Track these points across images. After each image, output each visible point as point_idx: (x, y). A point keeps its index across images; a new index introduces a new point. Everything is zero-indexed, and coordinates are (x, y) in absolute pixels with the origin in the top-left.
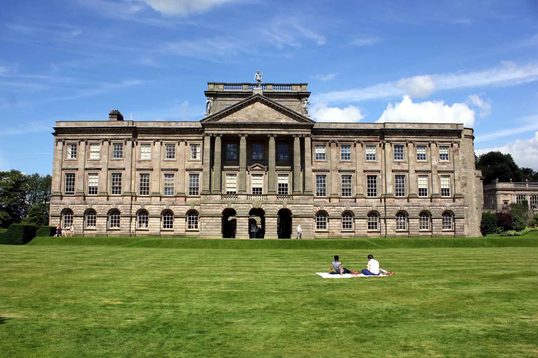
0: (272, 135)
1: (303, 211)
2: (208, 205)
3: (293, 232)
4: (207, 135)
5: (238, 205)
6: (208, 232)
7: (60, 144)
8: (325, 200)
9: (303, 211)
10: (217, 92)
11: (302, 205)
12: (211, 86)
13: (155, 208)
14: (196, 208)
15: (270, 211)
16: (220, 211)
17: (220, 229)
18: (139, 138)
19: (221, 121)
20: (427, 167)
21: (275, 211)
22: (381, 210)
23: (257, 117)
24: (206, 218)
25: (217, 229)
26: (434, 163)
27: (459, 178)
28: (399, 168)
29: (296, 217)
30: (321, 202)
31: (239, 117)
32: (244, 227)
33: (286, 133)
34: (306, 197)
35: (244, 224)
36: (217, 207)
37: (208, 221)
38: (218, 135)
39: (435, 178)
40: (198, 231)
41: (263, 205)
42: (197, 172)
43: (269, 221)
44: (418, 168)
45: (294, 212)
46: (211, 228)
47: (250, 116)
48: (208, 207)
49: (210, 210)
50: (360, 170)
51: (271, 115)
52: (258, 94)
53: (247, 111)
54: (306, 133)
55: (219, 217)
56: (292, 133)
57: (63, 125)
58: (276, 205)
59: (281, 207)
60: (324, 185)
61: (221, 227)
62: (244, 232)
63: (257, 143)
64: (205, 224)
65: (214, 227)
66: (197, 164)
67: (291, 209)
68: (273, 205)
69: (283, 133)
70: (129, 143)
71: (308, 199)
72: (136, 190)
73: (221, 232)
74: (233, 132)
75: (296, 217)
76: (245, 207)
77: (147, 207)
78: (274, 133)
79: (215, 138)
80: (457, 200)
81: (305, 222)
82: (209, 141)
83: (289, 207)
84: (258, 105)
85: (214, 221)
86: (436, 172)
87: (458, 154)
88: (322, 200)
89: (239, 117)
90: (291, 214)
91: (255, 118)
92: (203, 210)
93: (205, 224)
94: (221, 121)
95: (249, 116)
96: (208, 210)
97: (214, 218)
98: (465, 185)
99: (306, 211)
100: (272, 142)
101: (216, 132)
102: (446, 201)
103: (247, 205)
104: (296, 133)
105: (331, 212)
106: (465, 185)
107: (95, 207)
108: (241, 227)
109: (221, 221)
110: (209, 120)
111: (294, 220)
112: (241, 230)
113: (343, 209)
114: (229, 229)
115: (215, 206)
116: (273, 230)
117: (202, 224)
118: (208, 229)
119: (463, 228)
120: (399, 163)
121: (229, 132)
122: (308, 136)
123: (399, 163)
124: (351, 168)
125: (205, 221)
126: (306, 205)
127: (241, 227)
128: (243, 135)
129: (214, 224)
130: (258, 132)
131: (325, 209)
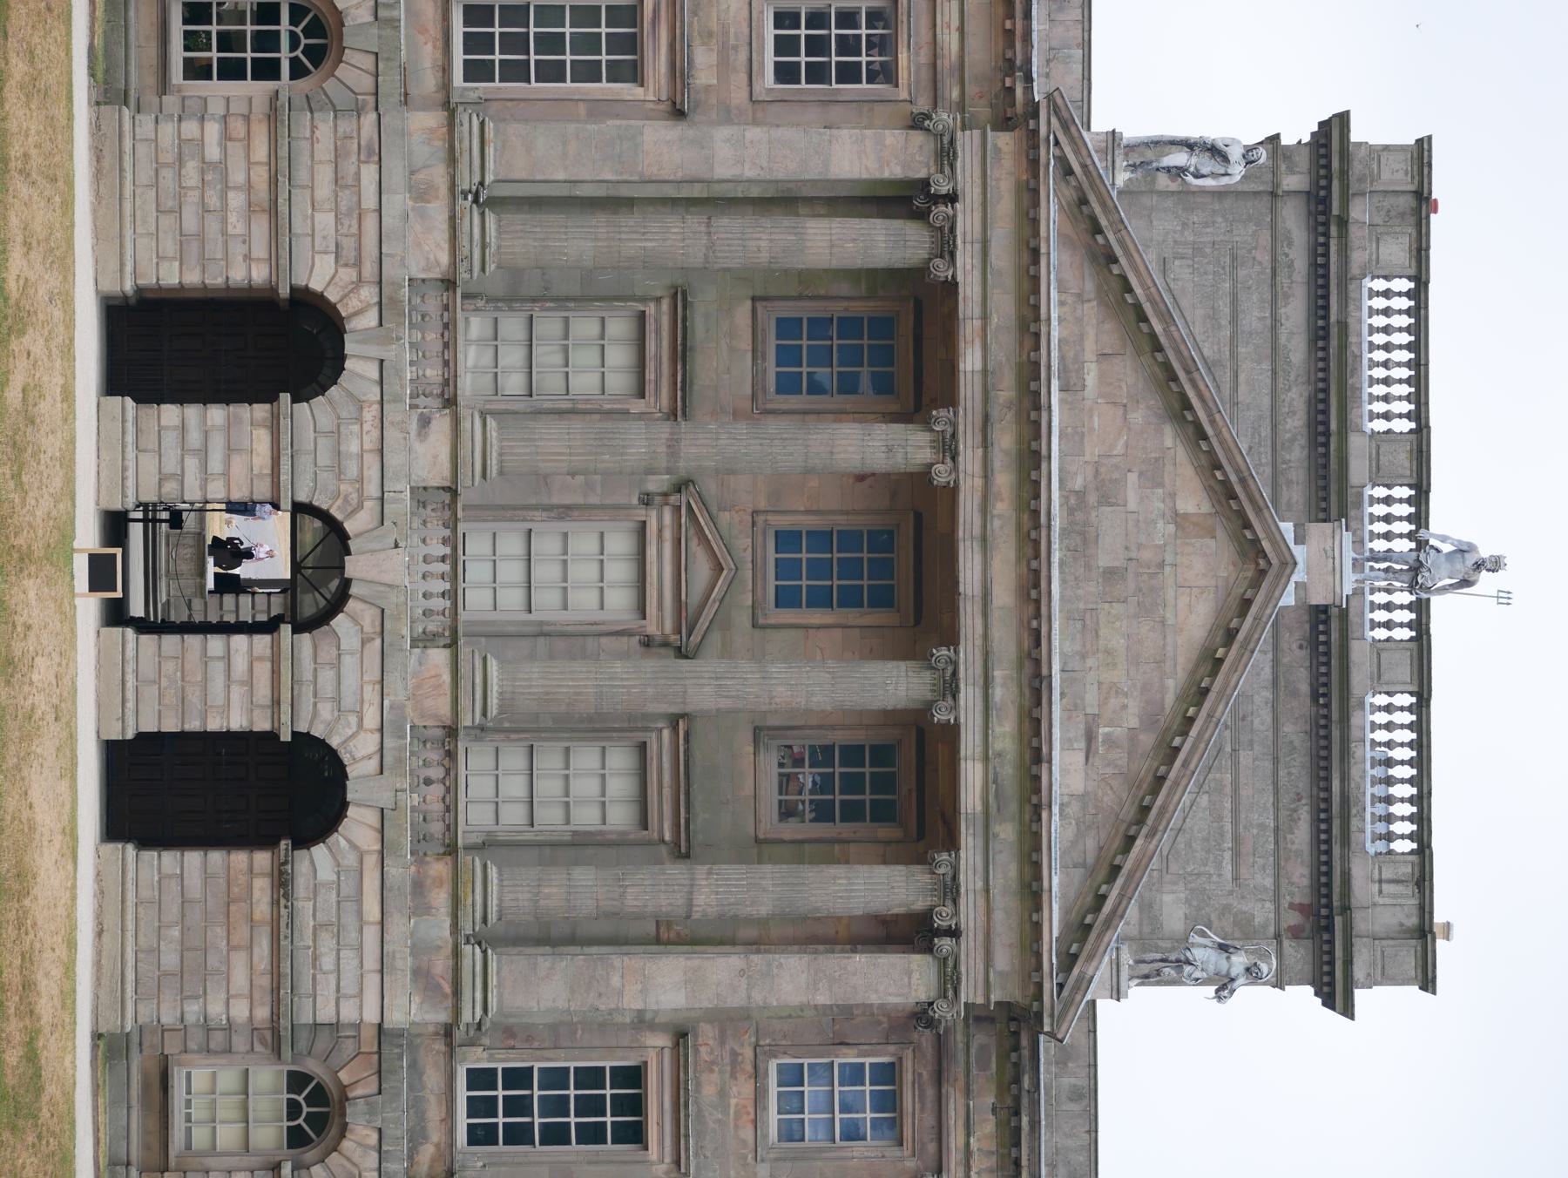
0: (951, 688)
1: (327, 943)
2: (369, 173)
3: (150, 856)
4: (946, 155)
5: (370, 414)
6: (145, 175)
8: (436, 1135)
9: (327, 943)
10: (1343, 222)
11: (371, 934)
12: (1396, 175)
14: (353, 71)
15: (327, 676)
16: (320, 274)
17: (170, 277)
19: (1060, 263)
21: (326, 711)
23: (1104, 561)
24: (261, 151)
25: (169, 246)
29: (282, 882)
30: (417, 1105)
31: (1096, 418)
32: (192, 464)
33: (971, 796)
34: (441, 965)
35: (216, 465)
36: (349, 244)
37: (237, 176)
38: (946, 247)
40: (164, 86)
41: (369, 618)
42: (657, 63)
43: (240, 664)
45: (317, 864)
47: (1105, 500)
48: (349, 167)
49: (324, 190)
51: (1118, 675)
52: (1289, 563)
53: (1153, 476)
55: (274, 258)
58: (371, 719)
59: (359, 752)
60: (557, 1135)
61: (193, 278)
62: (149, 463)
63: (893, 565)
64: (213, 152)
65: (190, 224)
66: (724, 65)
67: (337, 839)
68: (371, 694)
69: (972, 776)
73: (148, 280)
74: (970, 361)
75: (282, 882)
76: (352, 469)
78: (969, 695)
79: (921, 216)
81: (239, 961)
82: (894, 171)
85: (236, 225)
88: (434, 1113)
89: (1096, 418)
90: (305, 840)
91: (1082, 538)
92: (325, 129)
93: (213, 152)
94: (1060, 263)
95: (1108, 494)
96: (325, 175)
97: (261, 227)
99: (327, 962)
100: (895, 685)
101: (967, 221)
103: (373, 489)
104: (970, 881)
108: (194, 439)
109: (238, 275)
110: (1068, 171)
111: (249, 867)
112: (170, 439)
114: (175, 346)
116: (171, 698)
117: (213, 130)
118: (168, 175)
121: (969, 328)
122: (949, 980)
125: (236, 149)
126: (371, 962)
127: (194, 439)
128: (948, 448)
129: (213, 225)
130: (982, 571)
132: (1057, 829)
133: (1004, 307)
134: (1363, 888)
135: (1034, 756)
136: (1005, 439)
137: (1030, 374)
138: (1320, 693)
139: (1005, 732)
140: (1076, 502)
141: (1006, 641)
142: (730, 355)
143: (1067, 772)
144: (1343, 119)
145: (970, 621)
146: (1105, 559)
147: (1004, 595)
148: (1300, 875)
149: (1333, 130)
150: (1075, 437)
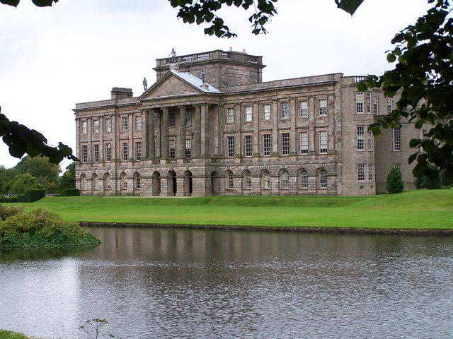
8: (233, 160)
13: (130, 172)
18: (120, 113)
20: (306, 124)
26: (312, 118)
27: (333, 133)
39: (312, 134)
44: (299, 125)
46: (147, 188)
50: (256, 131)
57: (79, 107)
59: (185, 169)
70: (114, 118)
71: (201, 162)
72: (121, 156)
77: (126, 171)
80: (329, 157)
83: (190, 169)
84: (173, 80)
87: (334, 107)
91: (171, 93)
98: (340, 140)
105: (235, 170)
106: (340, 140)
113: (243, 168)
115: (148, 169)
119: (335, 186)
124: (252, 129)
130: (173, 103)
131: (231, 168)
132: (192, 94)
133: (154, 103)
134: (211, 58)
135: (188, 97)
136: (164, 102)
137: (159, 100)
139: (184, 100)
141: (178, 101)
142: (172, 131)
143: (188, 93)
144: (154, 69)
145: (177, 104)
147: (174, 101)
148: (211, 66)
149: (156, 69)
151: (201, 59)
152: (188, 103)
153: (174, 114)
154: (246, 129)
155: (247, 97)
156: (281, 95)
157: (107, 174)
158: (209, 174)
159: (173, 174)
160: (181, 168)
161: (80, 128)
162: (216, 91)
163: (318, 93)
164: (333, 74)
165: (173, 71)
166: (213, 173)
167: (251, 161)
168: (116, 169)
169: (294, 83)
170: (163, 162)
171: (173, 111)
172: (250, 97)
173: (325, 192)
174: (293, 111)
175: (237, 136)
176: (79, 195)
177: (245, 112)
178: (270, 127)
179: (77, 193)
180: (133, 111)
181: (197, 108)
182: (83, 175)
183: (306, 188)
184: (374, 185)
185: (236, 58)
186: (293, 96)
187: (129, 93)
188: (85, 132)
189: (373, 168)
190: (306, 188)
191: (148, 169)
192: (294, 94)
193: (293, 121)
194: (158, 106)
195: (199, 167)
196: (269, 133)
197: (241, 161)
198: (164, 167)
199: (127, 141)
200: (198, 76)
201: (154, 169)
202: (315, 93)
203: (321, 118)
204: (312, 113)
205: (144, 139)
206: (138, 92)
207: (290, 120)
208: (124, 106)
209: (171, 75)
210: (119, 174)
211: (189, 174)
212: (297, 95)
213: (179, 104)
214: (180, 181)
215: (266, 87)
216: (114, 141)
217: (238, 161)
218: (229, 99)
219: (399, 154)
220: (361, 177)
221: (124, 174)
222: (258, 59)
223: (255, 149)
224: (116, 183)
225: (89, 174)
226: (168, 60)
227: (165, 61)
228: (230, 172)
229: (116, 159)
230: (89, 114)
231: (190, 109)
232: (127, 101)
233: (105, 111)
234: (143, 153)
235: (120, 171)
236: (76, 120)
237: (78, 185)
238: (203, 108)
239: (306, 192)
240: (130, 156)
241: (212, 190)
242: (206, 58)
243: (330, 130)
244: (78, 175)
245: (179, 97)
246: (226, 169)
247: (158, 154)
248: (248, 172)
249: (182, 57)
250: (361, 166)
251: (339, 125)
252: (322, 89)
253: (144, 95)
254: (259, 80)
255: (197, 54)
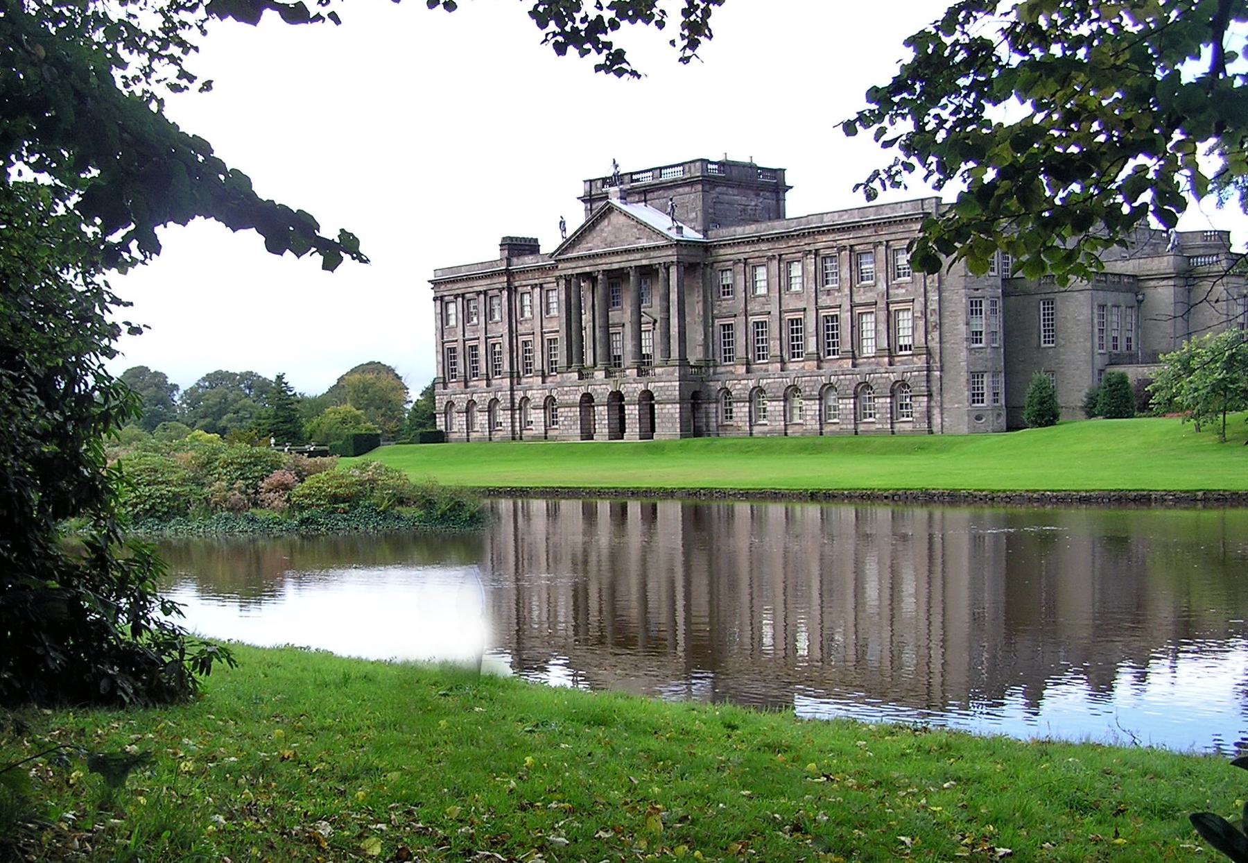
7: (439, 302)
13: (537, 396)
18: (516, 284)
22: (800, 383)
28: (828, 303)
31: (593, 244)
39: (882, 316)
44: (857, 299)
46: (569, 424)
50: (775, 312)
54: (675, 259)
56: (655, 261)
57: (440, 276)
59: (641, 387)
70: (505, 293)
77: (529, 394)
83: (651, 387)
84: (615, 218)
86: (884, 306)
91: (611, 244)
102: (903, 363)
107: (475, 398)
113: (751, 384)
120: (829, 292)
123: (829, 292)
124: (767, 309)
130: (616, 263)
131: (729, 385)
132: (652, 244)
133: (581, 263)
136: (599, 261)
137: (590, 257)
138: (660, 189)
139: (638, 256)
140: (607, 246)
141: (625, 257)
143: (644, 243)
145: (622, 265)
146: (611, 238)
147: (618, 259)
148: (687, 189)
150: (598, 247)
151: (668, 176)
152: (644, 262)
153: (618, 284)
154: (757, 309)
155: (757, 247)
156: (822, 242)
157: (495, 401)
158: (688, 395)
159: (617, 400)
160: (632, 387)
161: (443, 317)
162: (698, 237)
163: (893, 237)
164: (922, 200)
165: (615, 201)
166: (695, 396)
167: (767, 370)
168: (512, 390)
169: (846, 219)
170: (600, 375)
171: (616, 278)
172: (764, 246)
173: (908, 427)
174: (845, 273)
175: (739, 323)
176: (443, 442)
177: (754, 276)
178: (802, 305)
179: (441, 438)
180: (541, 281)
181: (662, 271)
182: (450, 404)
183: (872, 420)
184: (1004, 413)
185: (735, 172)
186: (845, 243)
187: (531, 246)
188: (452, 322)
189: (1002, 378)
190: (872, 420)
191: (569, 388)
192: (845, 239)
193: (847, 291)
194: (588, 269)
195: (667, 383)
196: (800, 315)
197: (748, 371)
198: (601, 386)
199: (530, 338)
200: (662, 209)
201: (583, 390)
202: (888, 238)
203: (899, 286)
204: (882, 276)
205: (563, 332)
206: (550, 243)
207: (839, 290)
208: (523, 271)
209: (610, 209)
210: (517, 401)
211: (647, 398)
212: (852, 242)
213: (628, 264)
214: (632, 412)
215: (793, 226)
216: (506, 338)
217: (742, 370)
218: (722, 251)
219: (1051, 352)
220: (976, 397)
221: (526, 399)
222: (778, 173)
223: (774, 347)
224: (513, 417)
225: (461, 401)
226: (604, 181)
227: (599, 184)
228: (728, 392)
229: (512, 373)
230: (459, 288)
231: (648, 273)
232: (529, 261)
233: (488, 282)
234: (561, 359)
235: (519, 395)
236: (435, 299)
237: (440, 423)
238: (673, 270)
239: (873, 427)
240: (537, 365)
241: (694, 426)
242: (678, 174)
243: (918, 306)
244: (440, 405)
245: (627, 251)
246: (719, 385)
247: (589, 360)
248: (760, 390)
249: (632, 174)
250: (975, 376)
251: (934, 297)
252: (901, 228)
253: (563, 249)
254: (779, 213)
255: (661, 169)
